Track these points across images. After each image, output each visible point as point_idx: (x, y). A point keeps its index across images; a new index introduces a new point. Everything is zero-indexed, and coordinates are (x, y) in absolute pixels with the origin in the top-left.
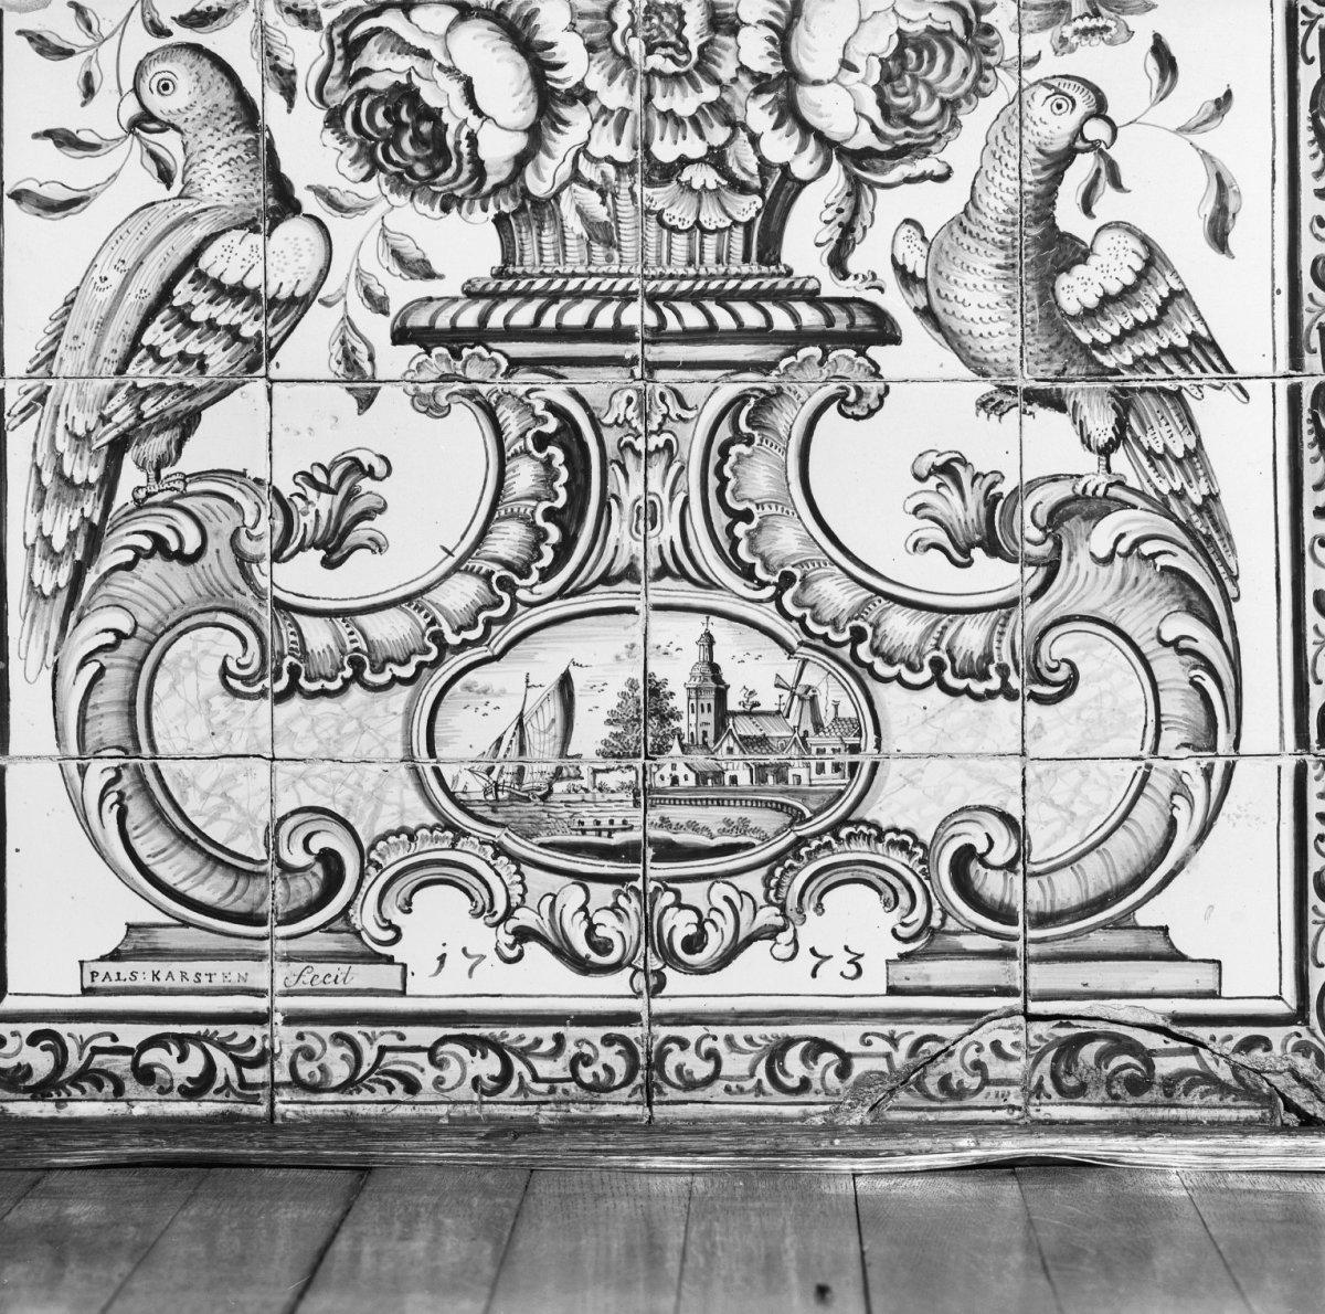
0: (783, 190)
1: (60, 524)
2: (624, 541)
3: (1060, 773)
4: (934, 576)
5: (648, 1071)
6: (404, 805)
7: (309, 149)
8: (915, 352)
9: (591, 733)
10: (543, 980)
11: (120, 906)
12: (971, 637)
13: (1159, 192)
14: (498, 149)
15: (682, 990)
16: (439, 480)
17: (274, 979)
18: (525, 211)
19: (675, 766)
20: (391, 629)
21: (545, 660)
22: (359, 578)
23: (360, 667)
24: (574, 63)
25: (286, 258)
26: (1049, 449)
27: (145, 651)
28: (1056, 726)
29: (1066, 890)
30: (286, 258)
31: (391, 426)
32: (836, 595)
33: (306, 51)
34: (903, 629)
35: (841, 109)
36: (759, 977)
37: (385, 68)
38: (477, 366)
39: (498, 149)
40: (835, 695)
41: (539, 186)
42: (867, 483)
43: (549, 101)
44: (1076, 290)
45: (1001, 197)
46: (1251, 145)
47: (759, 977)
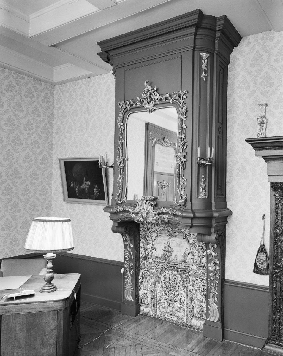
0: (174, 297)
1: (158, 302)
2: (171, 306)
3: (181, 315)
4: (178, 309)
5: (171, 320)
6: (165, 312)
7: (164, 294)
8: (177, 302)
9: (170, 311)
10: (168, 317)
11: (159, 313)
12: (179, 311)
13: (183, 300)
14: (168, 295)
15: (172, 319)
16: (166, 304)
17: (163, 316)
18: (168, 297)
19: (172, 312)
20: (165, 307)
21: (169, 309)
22: (165, 306)
23: (165, 308)
24: (170, 293)
25: (163, 297)
26: (180, 306)
27: (160, 306)
28: (181, 314)
29: (181, 318)
30: (163, 297)
31: (165, 302)
32: (175, 309)
33: (164, 291)
34: (177, 310)
35: (176, 295)
36: (173, 319)
37: (165, 292)
38: (167, 301)
39: (168, 295)
40: (175, 311)
41: (169, 296)
42: (177, 305)
43: (169, 294)
44: (181, 302)
45: (179, 299)
46: (185, 299)
47: (173, 319)
